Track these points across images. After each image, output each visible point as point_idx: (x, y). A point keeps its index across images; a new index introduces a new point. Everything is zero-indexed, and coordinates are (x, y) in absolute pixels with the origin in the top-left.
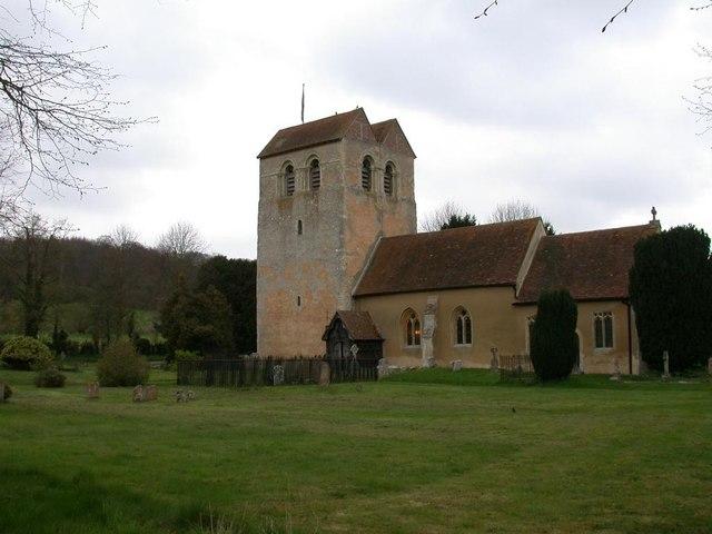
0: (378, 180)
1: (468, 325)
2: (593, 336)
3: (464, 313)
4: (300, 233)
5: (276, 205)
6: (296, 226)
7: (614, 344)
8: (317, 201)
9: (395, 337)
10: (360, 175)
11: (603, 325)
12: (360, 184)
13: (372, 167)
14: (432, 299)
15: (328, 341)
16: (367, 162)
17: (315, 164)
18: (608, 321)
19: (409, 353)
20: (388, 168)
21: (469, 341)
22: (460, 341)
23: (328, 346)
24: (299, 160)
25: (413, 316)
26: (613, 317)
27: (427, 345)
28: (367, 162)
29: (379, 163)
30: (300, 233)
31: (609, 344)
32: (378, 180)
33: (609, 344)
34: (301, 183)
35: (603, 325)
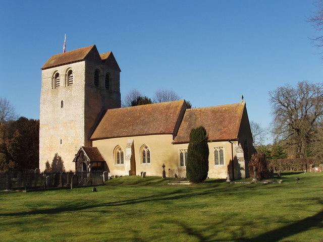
0: (102, 82)
1: (149, 154)
2: (214, 159)
3: (146, 147)
4: (62, 107)
5: (50, 93)
7: (224, 163)
9: (110, 160)
10: (93, 79)
11: (219, 153)
12: (93, 83)
13: (99, 75)
14: (130, 140)
15: (76, 162)
16: (97, 72)
17: (71, 72)
18: (221, 151)
19: (118, 168)
20: (107, 76)
21: (149, 161)
22: (144, 162)
23: (76, 165)
24: (62, 70)
25: (120, 149)
26: (224, 149)
27: (127, 164)
28: (97, 72)
29: (102, 73)
30: (62, 107)
31: (222, 162)
32: (102, 82)
33: (222, 162)
34: (62, 78)
35: (219, 153)
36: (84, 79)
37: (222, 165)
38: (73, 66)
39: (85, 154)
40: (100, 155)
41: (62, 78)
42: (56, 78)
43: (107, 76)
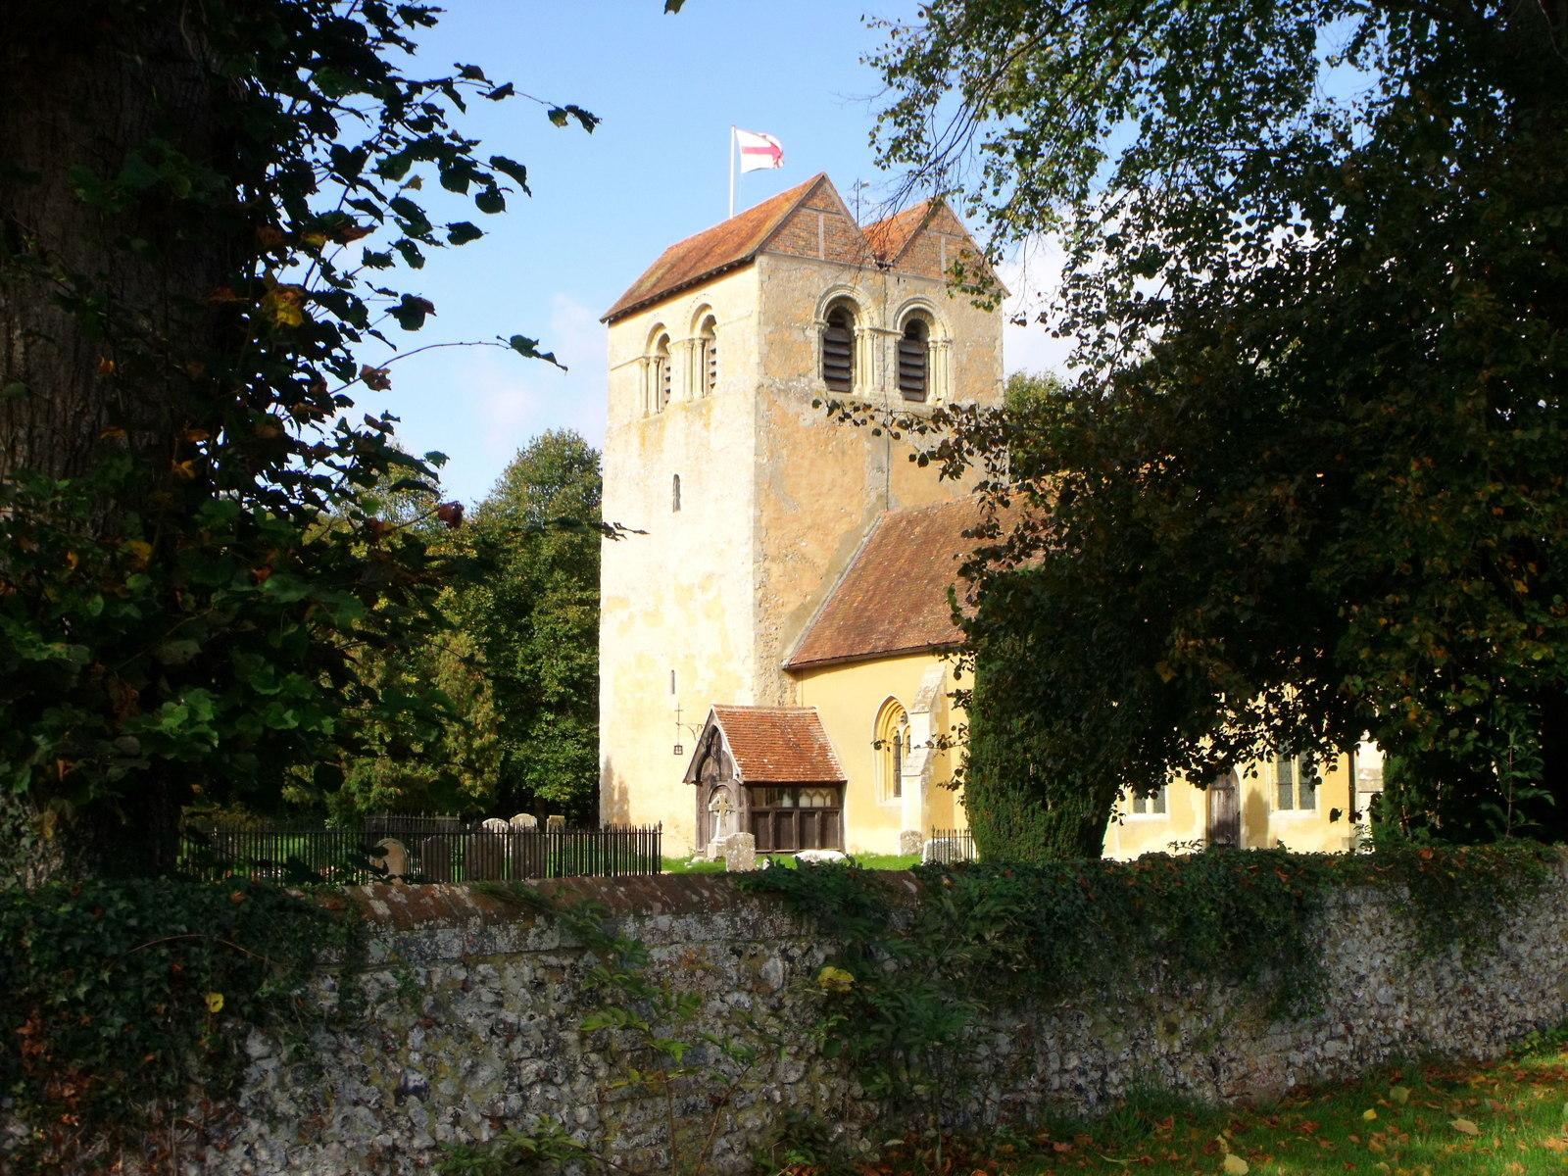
4: (677, 507)
5: (635, 441)
6: (671, 488)
8: (706, 426)
10: (815, 347)
15: (698, 782)
16: (840, 316)
24: (676, 315)
28: (840, 316)
30: (677, 507)
36: (755, 358)
37: (1306, 813)
38: (715, 294)
39: (726, 747)
40: (824, 749)
41: (678, 358)
42: (659, 360)
43: (915, 329)
